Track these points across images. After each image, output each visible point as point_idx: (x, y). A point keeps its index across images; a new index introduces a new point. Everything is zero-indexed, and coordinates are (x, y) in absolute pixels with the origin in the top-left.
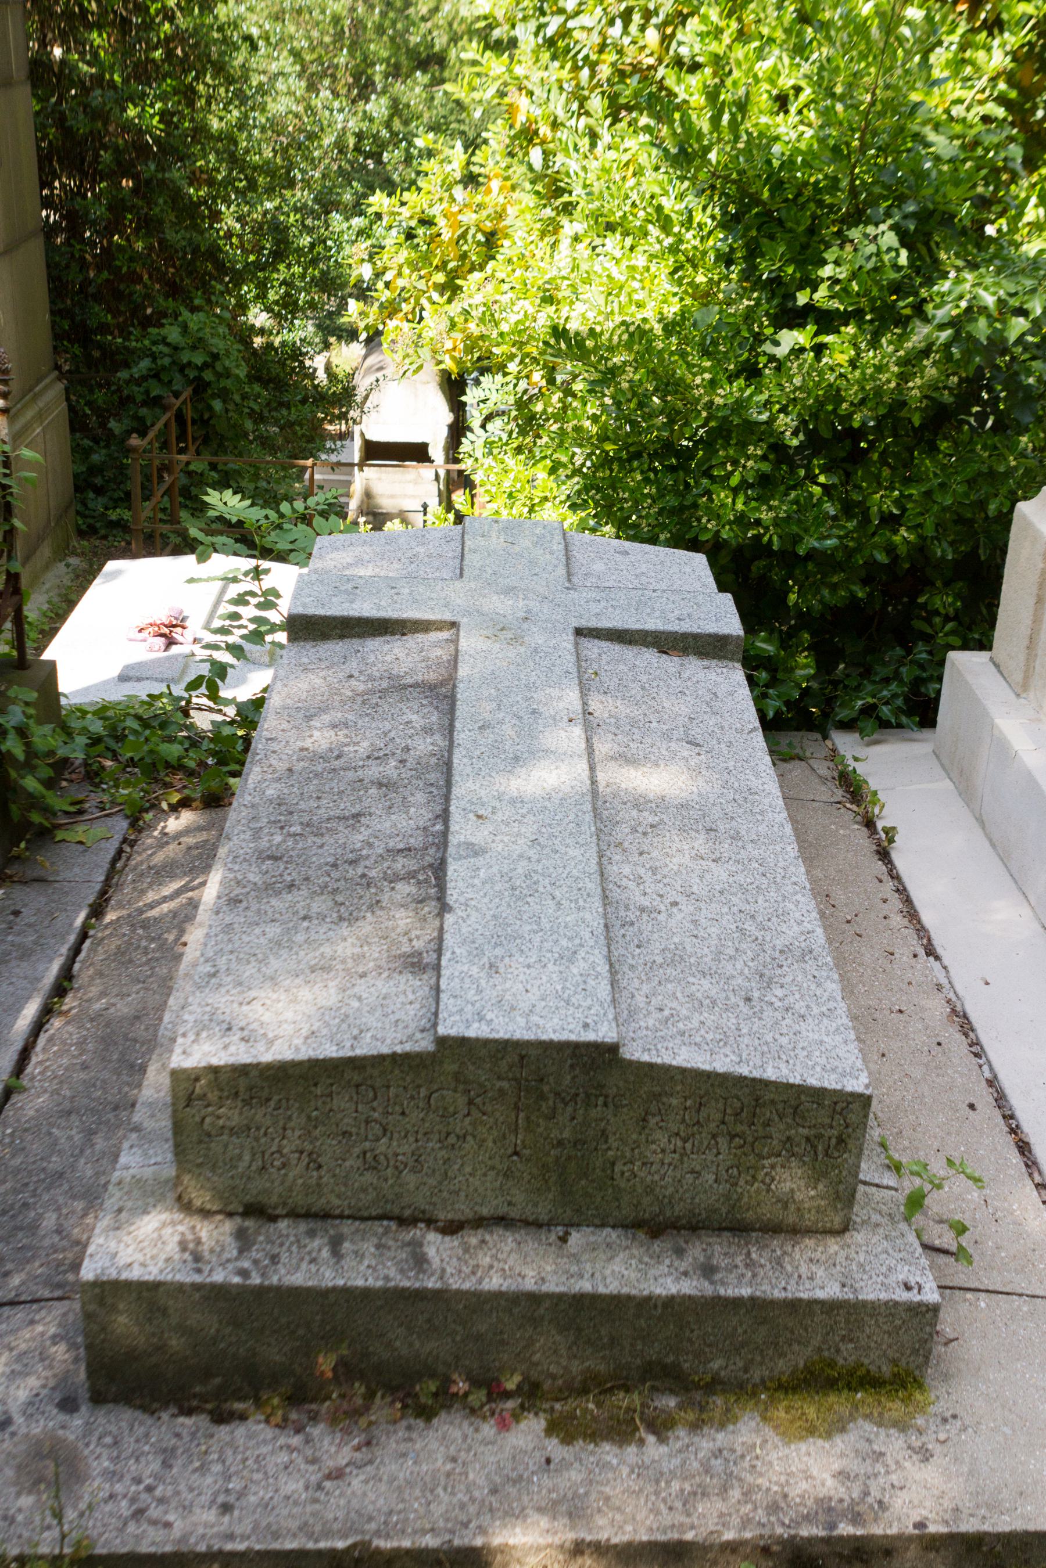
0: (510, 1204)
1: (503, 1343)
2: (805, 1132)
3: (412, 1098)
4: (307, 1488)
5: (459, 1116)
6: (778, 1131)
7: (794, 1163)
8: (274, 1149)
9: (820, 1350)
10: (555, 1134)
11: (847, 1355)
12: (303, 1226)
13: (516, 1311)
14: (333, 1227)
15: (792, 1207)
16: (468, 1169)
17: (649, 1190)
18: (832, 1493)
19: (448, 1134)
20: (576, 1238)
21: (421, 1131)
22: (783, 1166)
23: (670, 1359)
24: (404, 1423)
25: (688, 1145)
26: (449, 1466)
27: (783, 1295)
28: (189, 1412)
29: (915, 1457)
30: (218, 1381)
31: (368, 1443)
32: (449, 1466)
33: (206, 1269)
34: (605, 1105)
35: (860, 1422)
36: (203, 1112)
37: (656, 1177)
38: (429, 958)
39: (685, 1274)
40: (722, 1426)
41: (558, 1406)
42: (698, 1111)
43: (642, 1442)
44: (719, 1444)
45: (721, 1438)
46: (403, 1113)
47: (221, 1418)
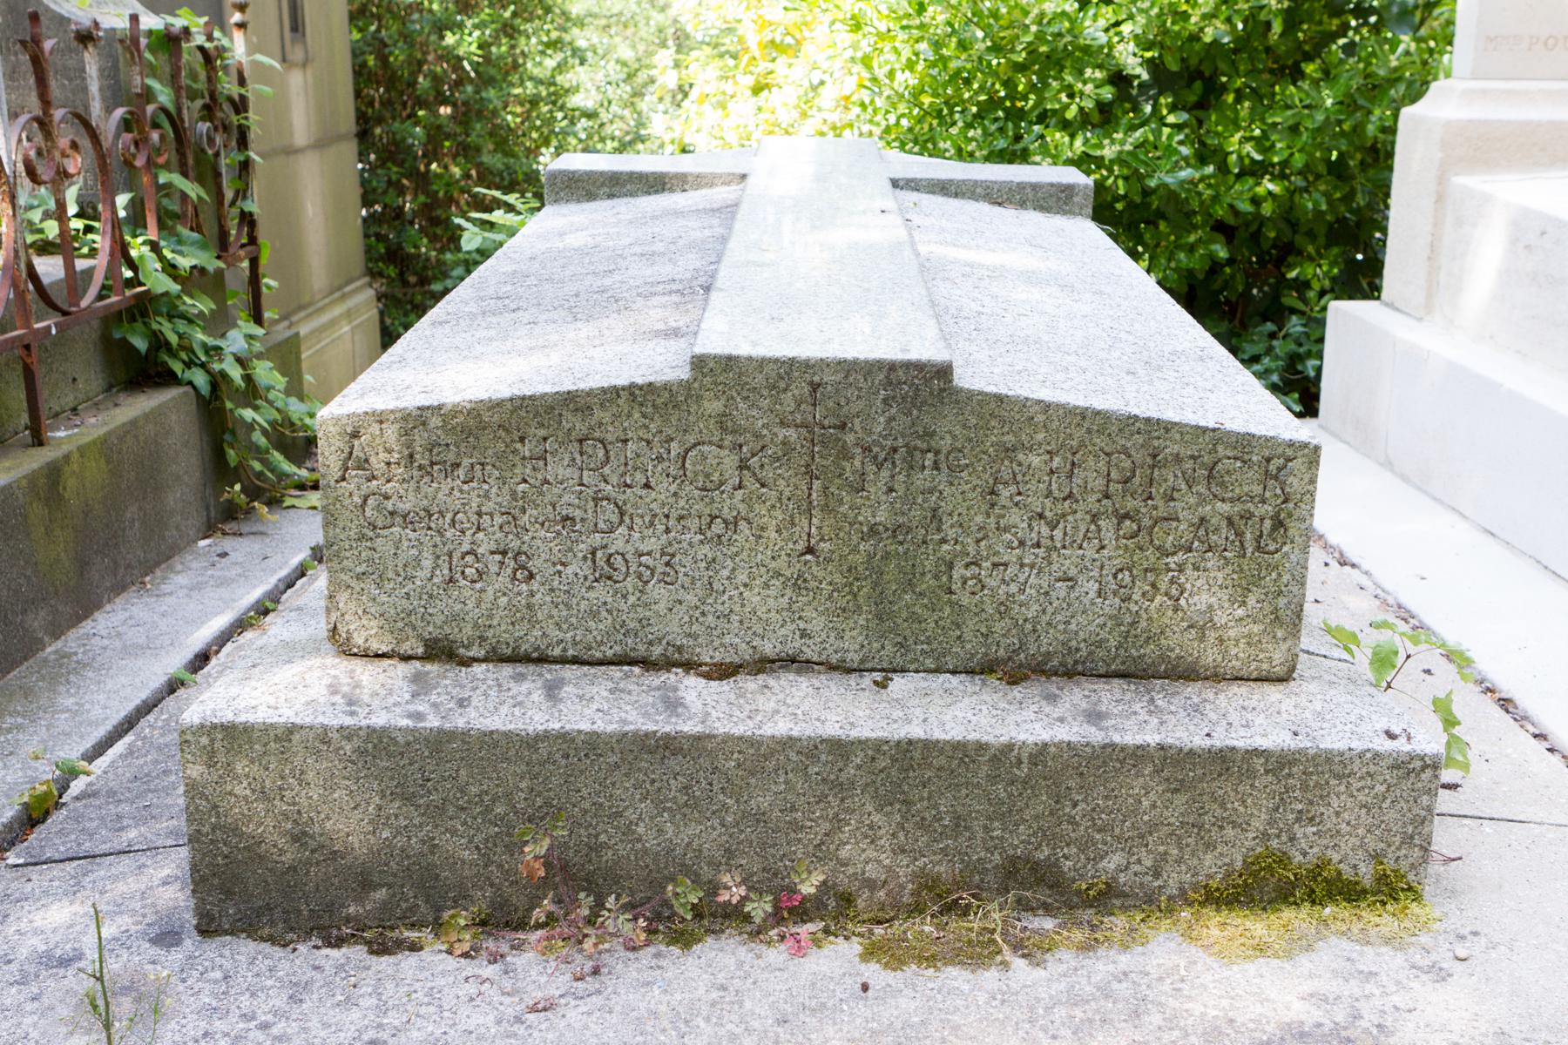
0: (804, 634)
1: (797, 827)
2: (1224, 508)
3: (660, 459)
4: (499, 1022)
5: (728, 488)
6: (1186, 508)
7: (1212, 561)
8: (466, 547)
9: (1265, 836)
10: (865, 515)
11: (1306, 847)
12: (507, 670)
13: (813, 770)
14: (549, 672)
15: (1212, 635)
16: (742, 577)
17: (1003, 610)
18: (1303, 1017)
19: (713, 518)
20: (898, 683)
21: (674, 514)
22: (1196, 568)
23: (1043, 854)
24: (651, 950)
25: (1058, 533)
26: (715, 995)
27: (1208, 742)
28: (339, 943)
29: (1424, 977)
30: (381, 894)
31: (596, 972)
32: (715, 995)
33: (362, 712)
34: (936, 467)
35: (1334, 940)
36: (364, 491)
37: (1013, 588)
38: (693, 328)
39: (1062, 720)
40: (1125, 947)
41: (879, 931)
42: (1070, 476)
43: (1005, 965)
44: (1122, 967)
45: (1125, 960)
46: (647, 486)
47: (381, 948)
